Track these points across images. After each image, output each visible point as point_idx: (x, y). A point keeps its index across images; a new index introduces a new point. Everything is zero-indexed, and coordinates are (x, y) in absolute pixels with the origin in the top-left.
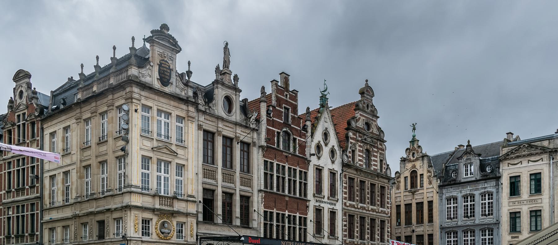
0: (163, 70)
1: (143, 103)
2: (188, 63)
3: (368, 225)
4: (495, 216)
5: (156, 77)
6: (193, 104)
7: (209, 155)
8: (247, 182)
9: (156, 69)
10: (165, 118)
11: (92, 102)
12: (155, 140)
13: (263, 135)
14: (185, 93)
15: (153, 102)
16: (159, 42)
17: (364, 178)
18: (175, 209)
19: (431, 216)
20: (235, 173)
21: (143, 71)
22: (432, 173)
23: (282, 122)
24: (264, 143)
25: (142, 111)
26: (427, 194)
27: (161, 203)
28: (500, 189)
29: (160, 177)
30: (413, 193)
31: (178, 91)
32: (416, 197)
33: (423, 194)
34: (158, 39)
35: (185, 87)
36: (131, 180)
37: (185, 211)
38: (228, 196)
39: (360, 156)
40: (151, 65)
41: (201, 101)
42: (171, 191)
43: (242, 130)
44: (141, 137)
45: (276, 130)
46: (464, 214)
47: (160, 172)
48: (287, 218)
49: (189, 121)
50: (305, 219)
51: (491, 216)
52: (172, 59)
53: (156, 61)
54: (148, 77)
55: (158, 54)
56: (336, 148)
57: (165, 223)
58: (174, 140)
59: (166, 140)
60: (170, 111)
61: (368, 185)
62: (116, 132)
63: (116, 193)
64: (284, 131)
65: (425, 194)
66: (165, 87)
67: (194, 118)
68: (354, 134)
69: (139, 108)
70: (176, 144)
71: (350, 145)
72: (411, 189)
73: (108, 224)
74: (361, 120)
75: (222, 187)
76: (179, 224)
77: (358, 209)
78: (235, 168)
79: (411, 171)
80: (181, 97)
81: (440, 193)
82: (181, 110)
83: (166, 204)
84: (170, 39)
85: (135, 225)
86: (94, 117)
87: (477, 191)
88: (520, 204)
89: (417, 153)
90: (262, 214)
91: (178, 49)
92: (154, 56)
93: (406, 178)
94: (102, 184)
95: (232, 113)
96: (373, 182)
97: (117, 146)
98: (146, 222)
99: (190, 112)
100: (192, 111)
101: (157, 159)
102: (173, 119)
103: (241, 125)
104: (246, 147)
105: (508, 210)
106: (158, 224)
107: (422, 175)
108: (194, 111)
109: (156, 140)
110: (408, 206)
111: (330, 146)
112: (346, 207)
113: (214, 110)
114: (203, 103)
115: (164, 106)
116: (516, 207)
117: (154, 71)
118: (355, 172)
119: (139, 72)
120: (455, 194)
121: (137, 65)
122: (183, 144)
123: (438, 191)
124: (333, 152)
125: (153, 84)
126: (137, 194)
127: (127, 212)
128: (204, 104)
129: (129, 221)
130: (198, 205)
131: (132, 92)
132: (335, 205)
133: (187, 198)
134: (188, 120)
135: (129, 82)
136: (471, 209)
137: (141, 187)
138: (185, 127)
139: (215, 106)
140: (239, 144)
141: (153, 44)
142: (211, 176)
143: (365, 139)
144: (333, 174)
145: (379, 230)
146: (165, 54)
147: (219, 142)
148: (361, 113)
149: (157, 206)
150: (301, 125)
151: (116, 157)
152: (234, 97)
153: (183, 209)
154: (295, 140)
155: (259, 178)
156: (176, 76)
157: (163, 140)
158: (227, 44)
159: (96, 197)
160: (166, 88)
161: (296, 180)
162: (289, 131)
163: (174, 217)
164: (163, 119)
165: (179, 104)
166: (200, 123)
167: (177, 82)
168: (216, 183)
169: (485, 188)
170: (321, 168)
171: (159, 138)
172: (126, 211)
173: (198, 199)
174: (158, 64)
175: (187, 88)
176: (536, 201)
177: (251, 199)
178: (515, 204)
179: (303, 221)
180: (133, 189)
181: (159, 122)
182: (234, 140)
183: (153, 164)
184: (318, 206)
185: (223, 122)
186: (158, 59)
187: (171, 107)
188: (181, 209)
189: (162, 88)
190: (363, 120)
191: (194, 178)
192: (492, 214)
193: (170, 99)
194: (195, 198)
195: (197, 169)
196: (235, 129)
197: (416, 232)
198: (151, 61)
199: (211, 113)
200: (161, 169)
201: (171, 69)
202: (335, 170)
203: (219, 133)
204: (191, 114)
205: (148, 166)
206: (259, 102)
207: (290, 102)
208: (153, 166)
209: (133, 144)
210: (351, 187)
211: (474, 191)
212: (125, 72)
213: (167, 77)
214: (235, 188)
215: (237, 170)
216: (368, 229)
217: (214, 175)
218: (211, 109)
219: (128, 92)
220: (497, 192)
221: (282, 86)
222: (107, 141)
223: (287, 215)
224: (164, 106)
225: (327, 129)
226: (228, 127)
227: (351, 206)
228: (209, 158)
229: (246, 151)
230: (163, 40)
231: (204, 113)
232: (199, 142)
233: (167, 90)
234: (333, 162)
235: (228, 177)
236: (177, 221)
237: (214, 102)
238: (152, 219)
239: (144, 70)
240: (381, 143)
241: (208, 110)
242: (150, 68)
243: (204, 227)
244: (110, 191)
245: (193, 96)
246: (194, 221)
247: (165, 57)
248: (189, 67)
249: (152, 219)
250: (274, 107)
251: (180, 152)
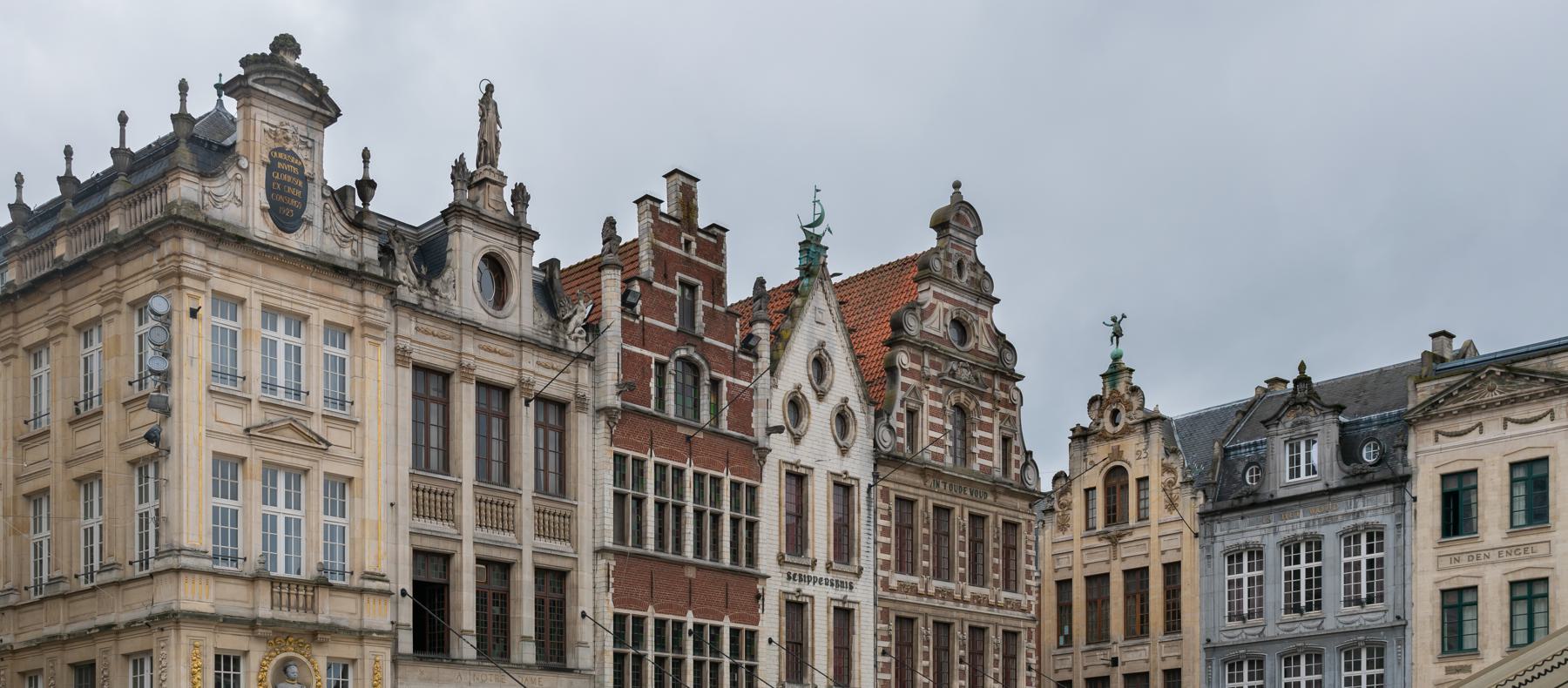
0: (279, 181)
1: (216, 288)
2: (363, 156)
3: (962, 647)
4: (1391, 603)
5: (257, 205)
6: (379, 284)
7: (434, 443)
8: (557, 524)
9: (258, 177)
10: (288, 332)
11: (52, 290)
12: (254, 403)
13: (611, 373)
14: (353, 252)
15: (248, 284)
16: (268, 94)
17: (948, 498)
18: (323, 619)
19: (1174, 612)
20: (517, 498)
21: (217, 186)
22: (1179, 472)
23: (674, 329)
24: (612, 400)
25: (214, 313)
26: (1159, 543)
27: (275, 602)
28: (1408, 514)
29: (274, 518)
30: (1114, 541)
31: (329, 246)
32: (1123, 551)
33: (1146, 542)
34: (264, 85)
35: (354, 231)
36: (180, 533)
37: (354, 624)
38: (497, 571)
39: (933, 427)
40: (240, 168)
41: (404, 274)
42: (308, 561)
43: (541, 360)
44: (209, 396)
45: (654, 356)
46: (1286, 601)
47: (274, 504)
48: (690, 635)
49: (367, 339)
50: (752, 635)
51: (1376, 606)
52: (310, 144)
53: (258, 153)
54: (231, 204)
55: (265, 131)
56: (855, 405)
57: (291, 663)
58: (316, 403)
59: (291, 401)
60: (304, 310)
61: (960, 518)
62: (130, 383)
63: (129, 576)
64: (680, 359)
65: (1154, 540)
66: (287, 235)
67: (381, 328)
68: (914, 359)
69: (205, 304)
70: (325, 413)
71: (900, 394)
72: (1106, 527)
73: (105, 673)
74: (936, 313)
75: (474, 543)
76: (336, 666)
77: (930, 597)
78: (519, 481)
79: (1105, 470)
80: (341, 263)
81: (1205, 537)
82: (339, 304)
83: (293, 603)
84: (303, 80)
85: (193, 674)
86: (60, 339)
87: (1331, 526)
88: (1475, 561)
89: (1127, 411)
90: (609, 623)
91: (328, 113)
92: (252, 139)
93: (1090, 492)
94: (86, 550)
95: (508, 308)
96: (979, 508)
97: (133, 425)
98: (227, 662)
99: (370, 310)
100: (375, 305)
101: (264, 462)
102: (314, 333)
103: (537, 345)
104: (554, 411)
105: (1436, 583)
106: (266, 668)
107: (1143, 481)
108: (381, 306)
109: (261, 402)
110: (1098, 582)
111: (833, 400)
113: (449, 300)
114: (414, 279)
115: (283, 293)
116: (1461, 572)
117: (251, 186)
118: (919, 481)
119: (204, 192)
120: (1254, 539)
121: (196, 170)
122: (347, 411)
123: (1197, 531)
124: (843, 419)
125: (248, 228)
126: (197, 576)
127: (165, 634)
128: (417, 283)
129: (173, 663)
130: (397, 603)
131: (182, 254)
132: (851, 588)
133: (361, 581)
134: (363, 336)
135: (172, 224)
136: (1309, 584)
137: (211, 553)
138: (352, 357)
139: (451, 286)
140: (532, 404)
141: (248, 101)
142: (439, 511)
143: (953, 373)
144: (843, 488)
145: (997, 664)
146: (285, 129)
147: (465, 400)
148: (938, 290)
149: (265, 612)
150: (737, 337)
151: (128, 462)
152: (514, 255)
153: (345, 616)
154: (715, 384)
155: (598, 511)
156: (324, 196)
157: (283, 404)
158: (490, 88)
159: (66, 589)
160: (292, 236)
161: (721, 514)
162: (697, 357)
163: (320, 643)
164: (281, 335)
165: (335, 286)
166: (402, 343)
167: (327, 216)
168: (455, 531)
169: (1357, 514)
170: (803, 471)
171: (268, 397)
172: (162, 630)
173: (397, 584)
174: (264, 163)
175: (359, 233)
176: (1530, 551)
177: (571, 579)
178: (1457, 564)
179: (745, 643)
180: (185, 561)
181: (269, 347)
182: (516, 394)
183: (251, 478)
184: (793, 594)
185: (477, 337)
186: (264, 147)
187: (309, 296)
188: (341, 619)
189: (279, 240)
190: (946, 311)
191: (382, 519)
192: (1381, 598)
193: (304, 272)
194: (387, 581)
195: (392, 489)
196: (516, 359)
197: (1123, 663)
198: (240, 154)
199: (438, 310)
200: (274, 493)
201: (306, 177)
202: (850, 474)
203: (466, 372)
204: (373, 316)
205: (235, 487)
206: (596, 268)
207: (698, 264)
208: (251, 487)
209: (184, 418)
210: (904, 530)
211: (1320, 525)
212: (156, 193)
213: (294, 202)
214: (518, 547)
215: (524, 487)
216: (961, 661)
217: (450, 506)
218: (437, 298)
219: (169, 256)
220: (1398, 526)
221: (674, 214)
222: (100, 413)
223: (690, 626)
224: (283, 293)
225: (822, 345)
226: (495, 352)
227: (903, 587)
228: (434, 454)
229: (553, 428)
230: (279, 85)
231: (416, 309)
232: (399, 404)
233: (295, 242)
234: (844, 451)
235: (496, 513)
236: (328, 657)
237: (447, 275)
238: (246, 653)
239: (218, 183)
240: (1005, 382)
241: (429, 301)
242: (239, 176)
243: (418, 673)
244: (112, 569)
245: (380, 259)
246: (385, 654)
247: (287, 139)
248: (366, 167)
249: (246, 653)
250: (646, 283)
251: (336, 436)
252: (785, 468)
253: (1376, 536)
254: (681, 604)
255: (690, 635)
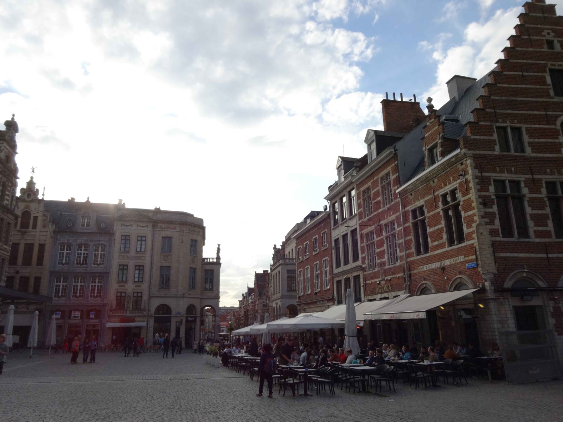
22: (48, 217)
30: (23, 233)
136: (84, 257)
192: (103, 264)
253: (104, 247)
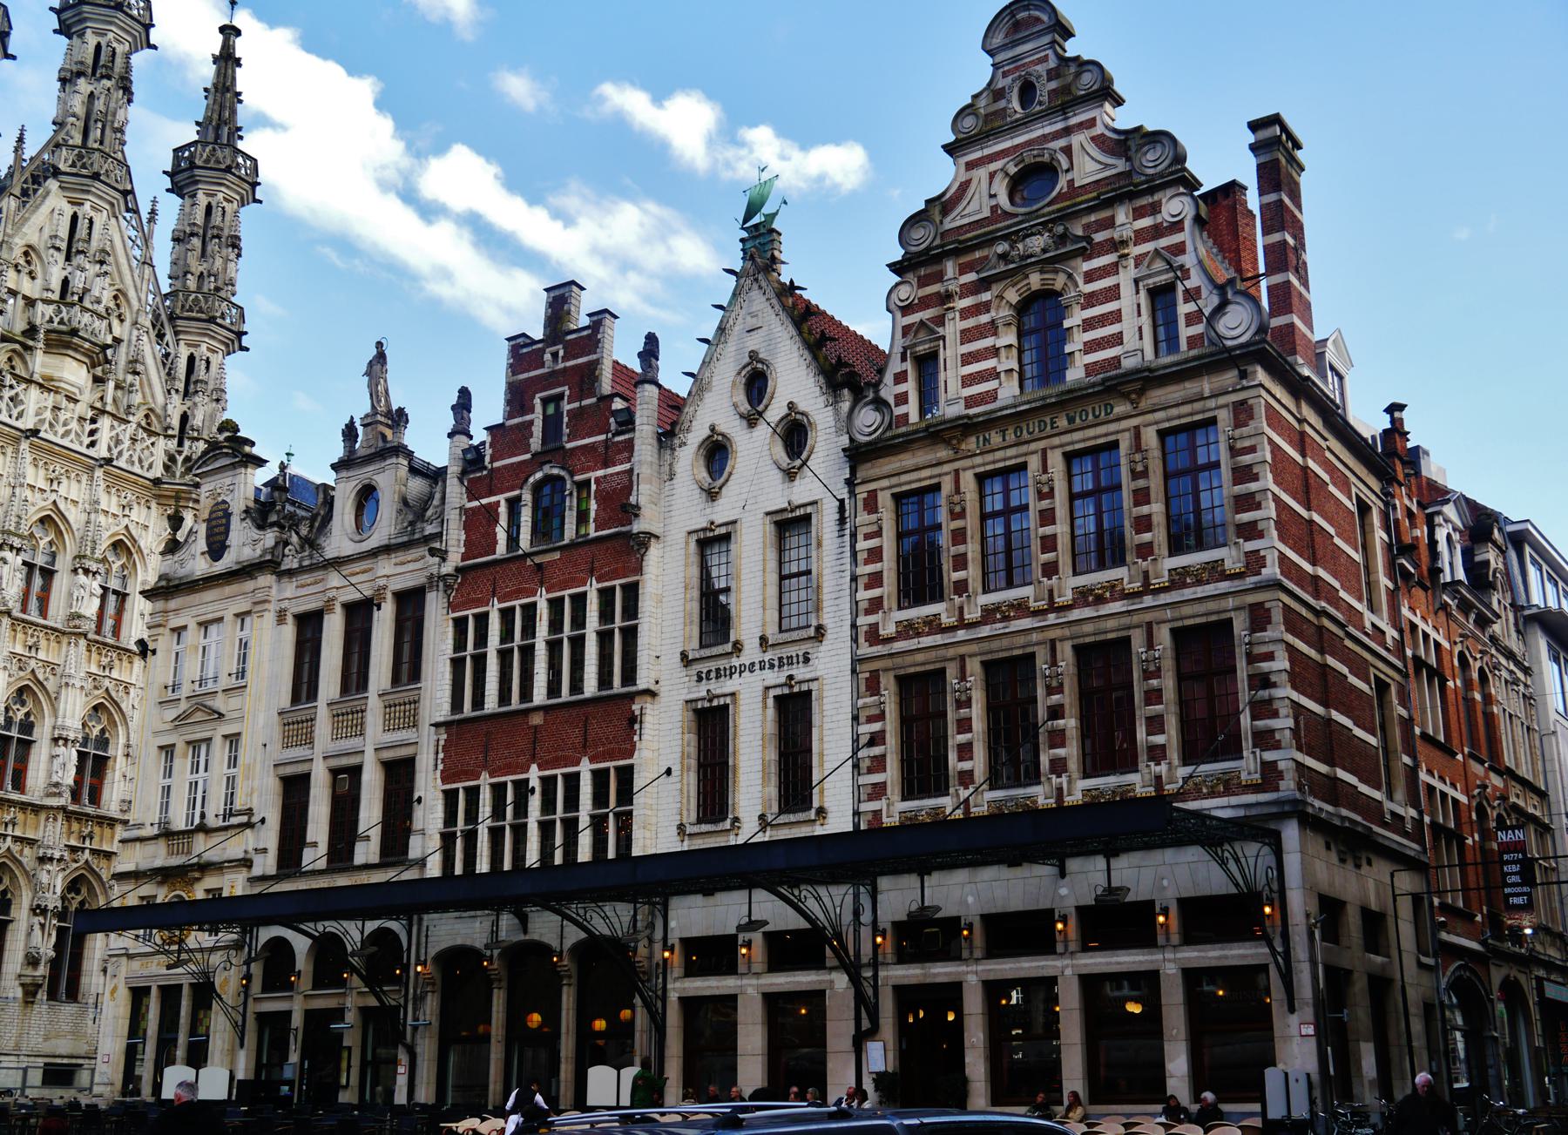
48: (533, 788)
75: (325, 758)
104: (410, 603)
112: (879, 648)
132: (807, 660)
170: (723, 530)
184: (703, 699)
202: (718, 522)
252: (695, 537)
254: (522, 760)
255: (533, 788)
